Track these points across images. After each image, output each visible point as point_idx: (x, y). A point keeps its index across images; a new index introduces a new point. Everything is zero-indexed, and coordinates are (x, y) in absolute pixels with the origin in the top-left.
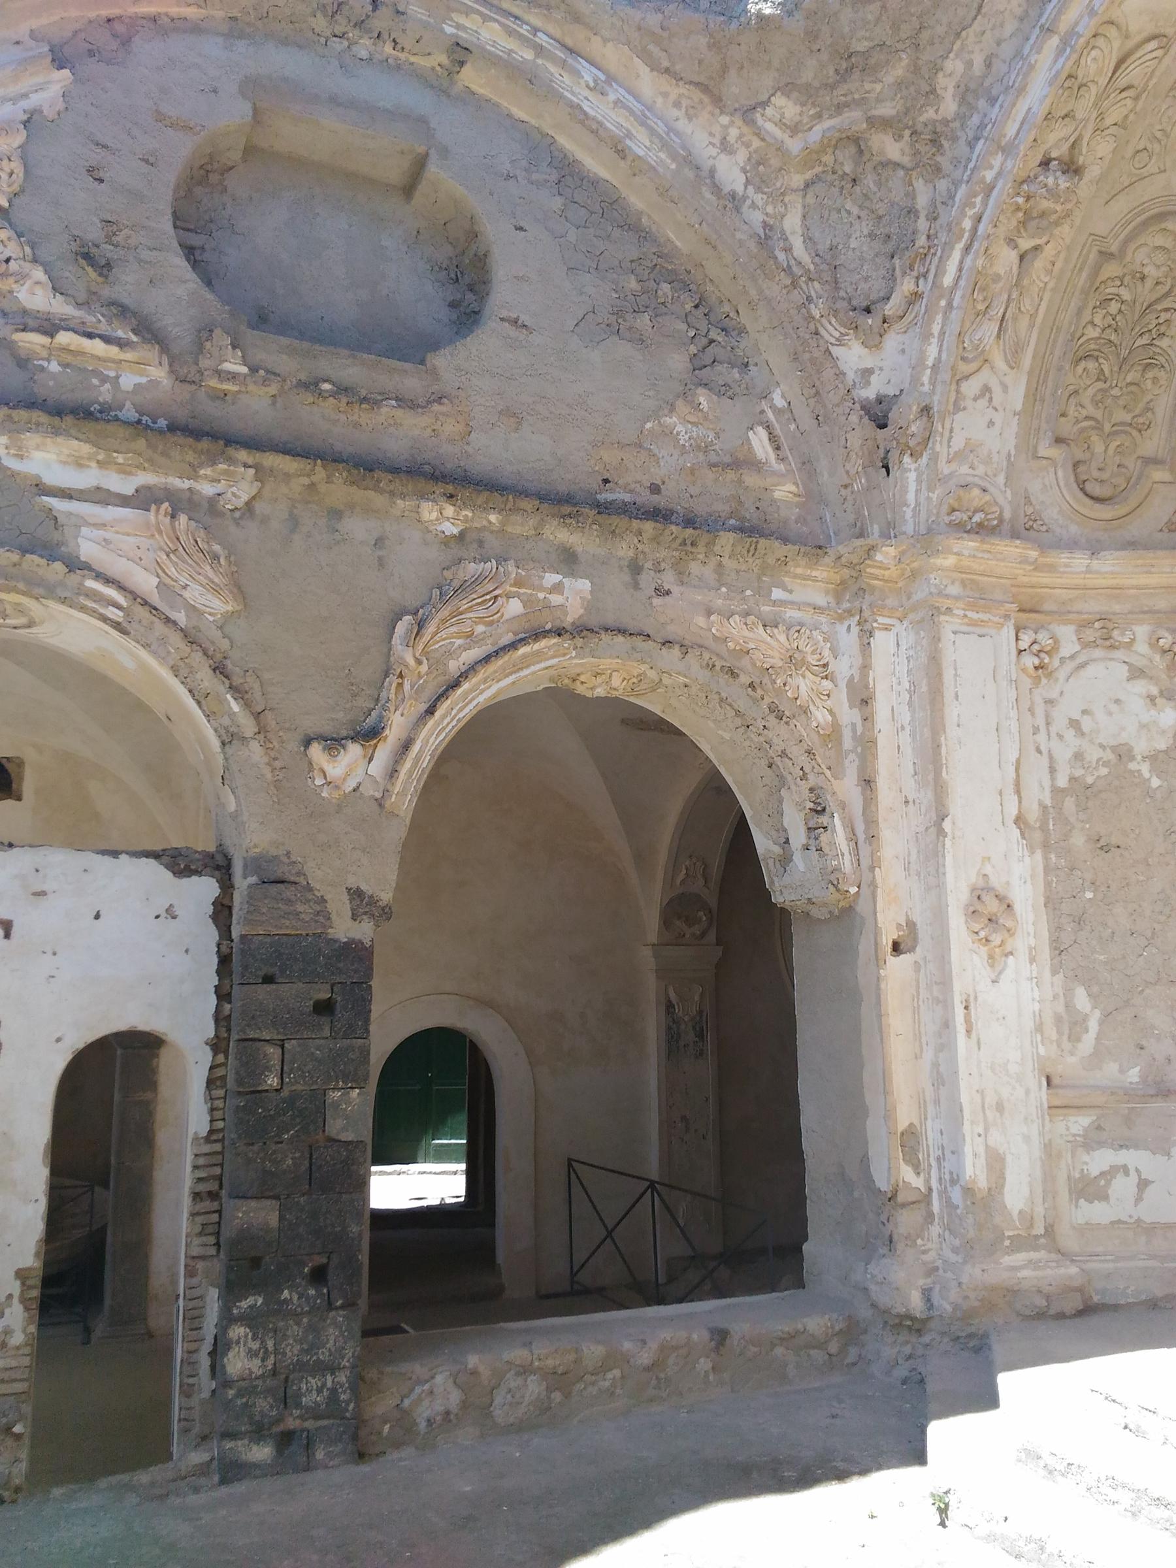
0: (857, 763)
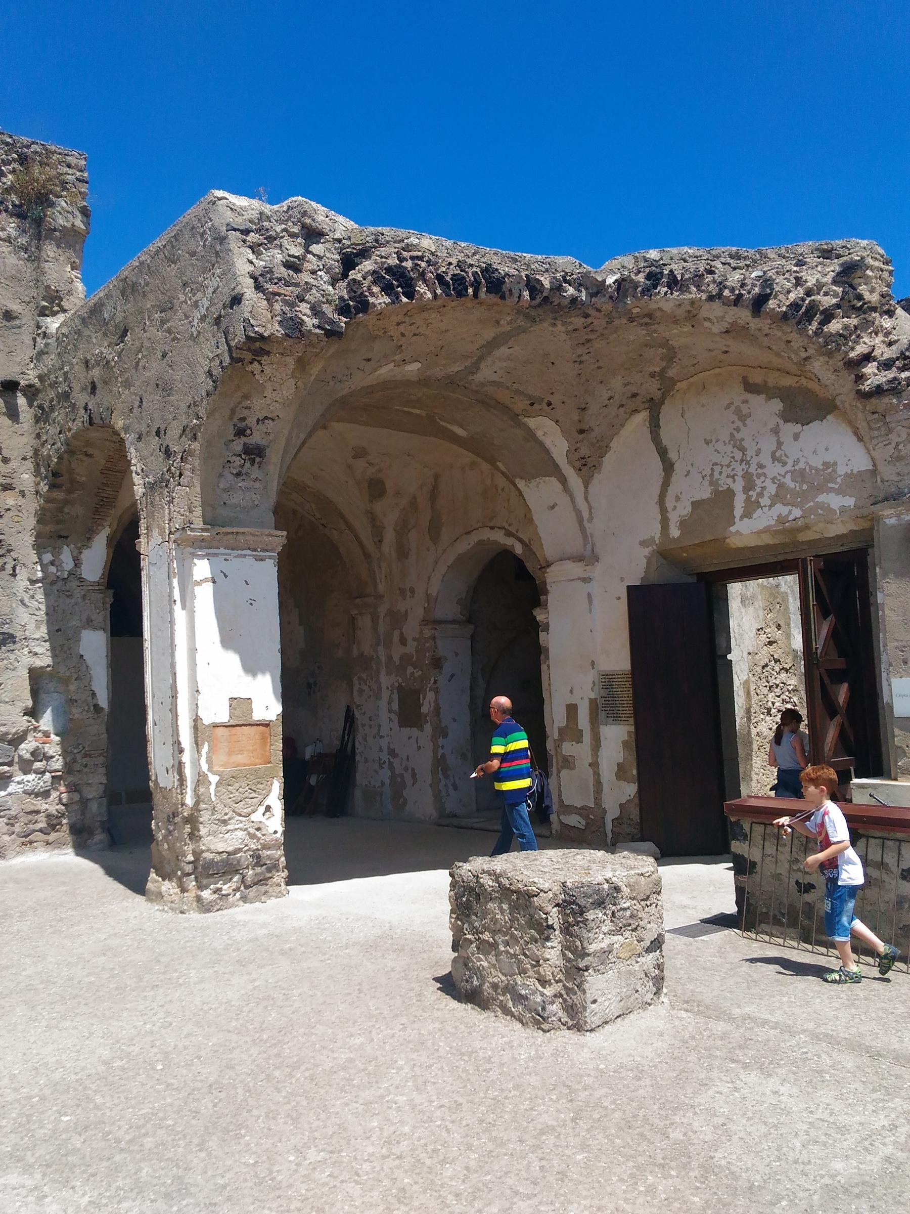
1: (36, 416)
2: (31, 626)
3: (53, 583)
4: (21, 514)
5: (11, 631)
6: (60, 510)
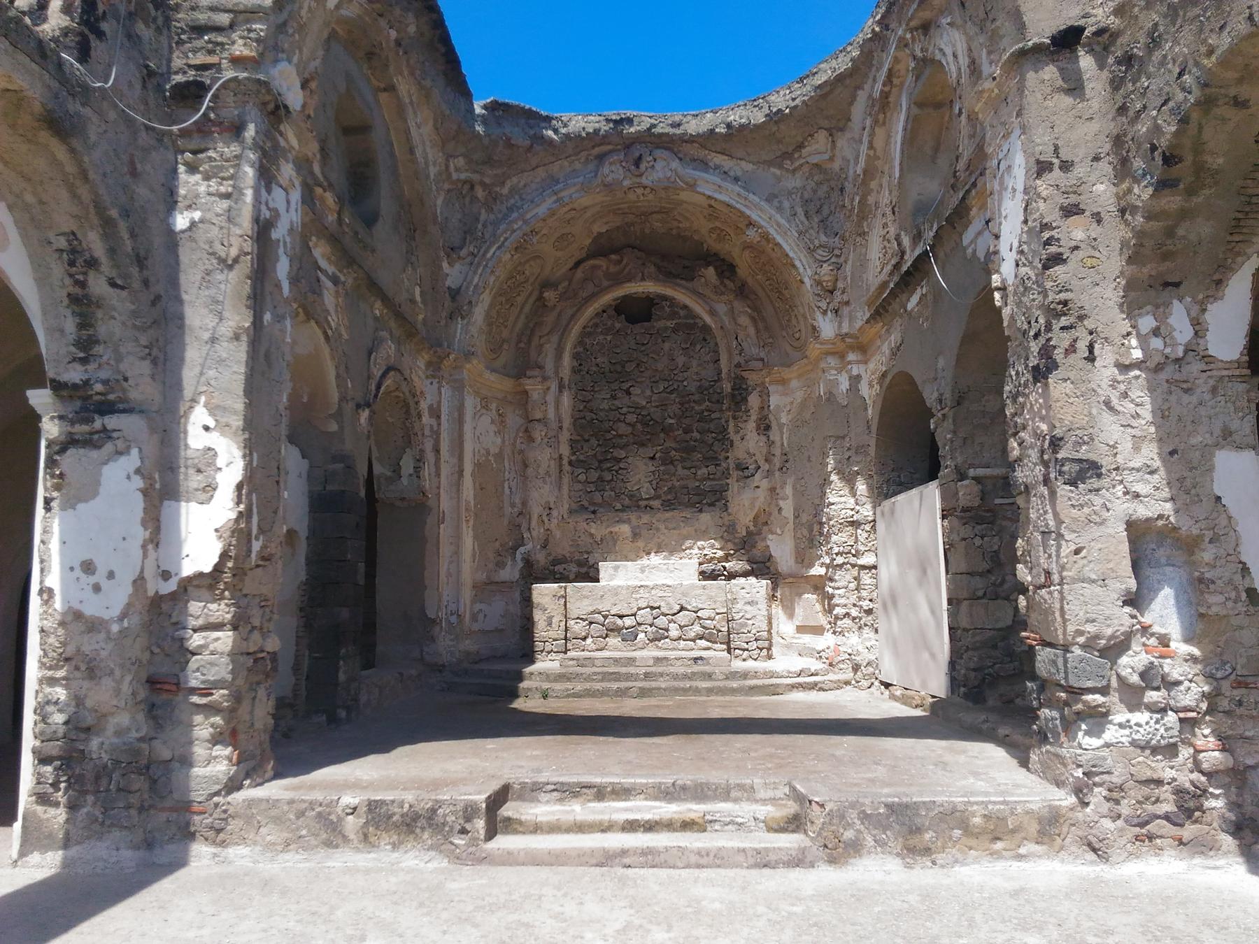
0: (432, 441)
2: (1126, 446)
3: (1158, 368)
4: (1097, 254)
6: (1170, 233)
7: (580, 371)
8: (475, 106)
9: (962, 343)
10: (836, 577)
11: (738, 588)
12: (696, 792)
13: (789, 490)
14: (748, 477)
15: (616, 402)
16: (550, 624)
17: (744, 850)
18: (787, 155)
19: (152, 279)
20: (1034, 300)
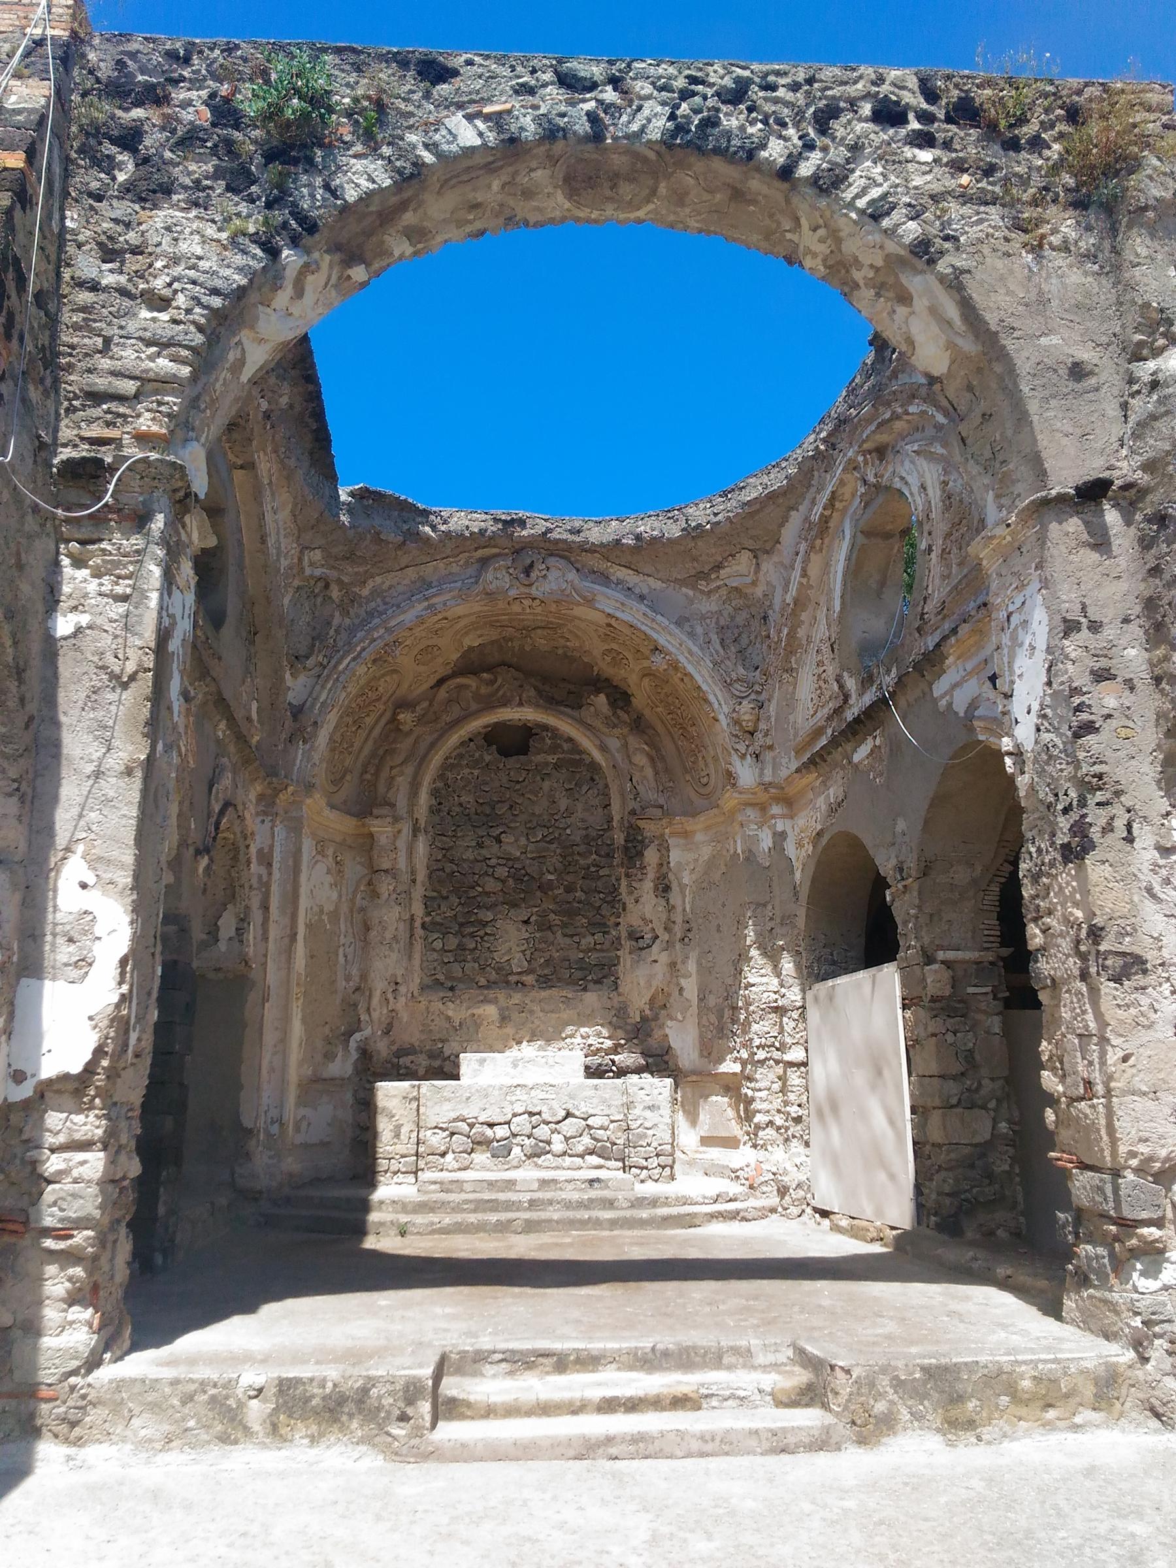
0: (260, 896)
1: (1141, 540)
4: (1131, 724)
5: (1136, 950)
7: (439, 811)
8: (340, 492)
9: (931, 806)
10: (758, 1076)
11: (636, 1089)
12: (681, 1359)
13: (692, 966)
14: (644, 949)
15: (484, 852)
16: (397, 1136)
17: (757, 1432)
18: (702, 575)
19: (28, 695)
20: (1062, 770)
